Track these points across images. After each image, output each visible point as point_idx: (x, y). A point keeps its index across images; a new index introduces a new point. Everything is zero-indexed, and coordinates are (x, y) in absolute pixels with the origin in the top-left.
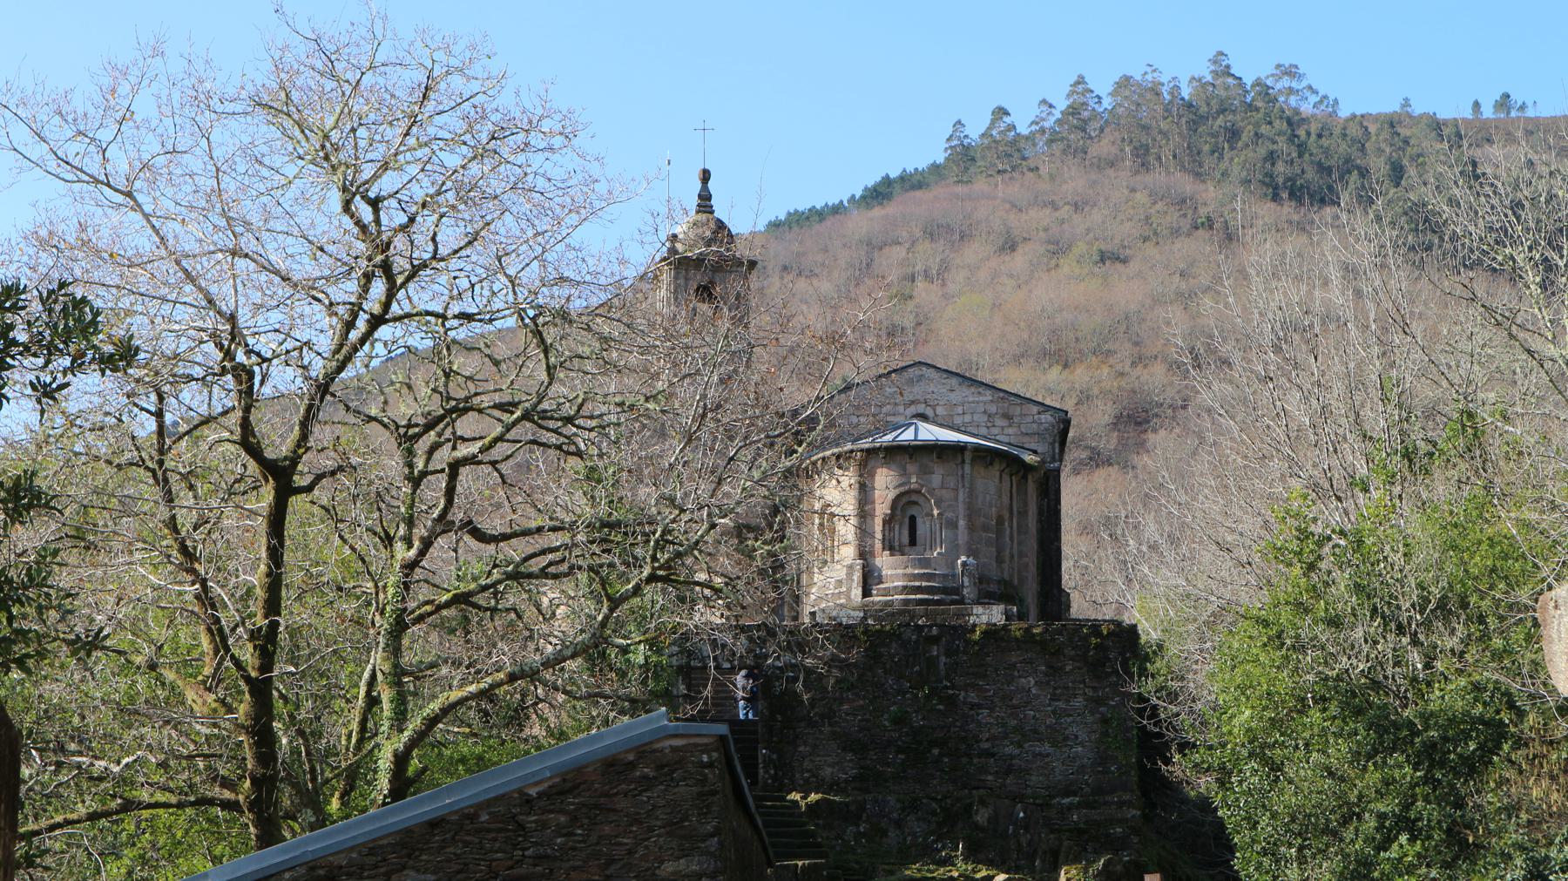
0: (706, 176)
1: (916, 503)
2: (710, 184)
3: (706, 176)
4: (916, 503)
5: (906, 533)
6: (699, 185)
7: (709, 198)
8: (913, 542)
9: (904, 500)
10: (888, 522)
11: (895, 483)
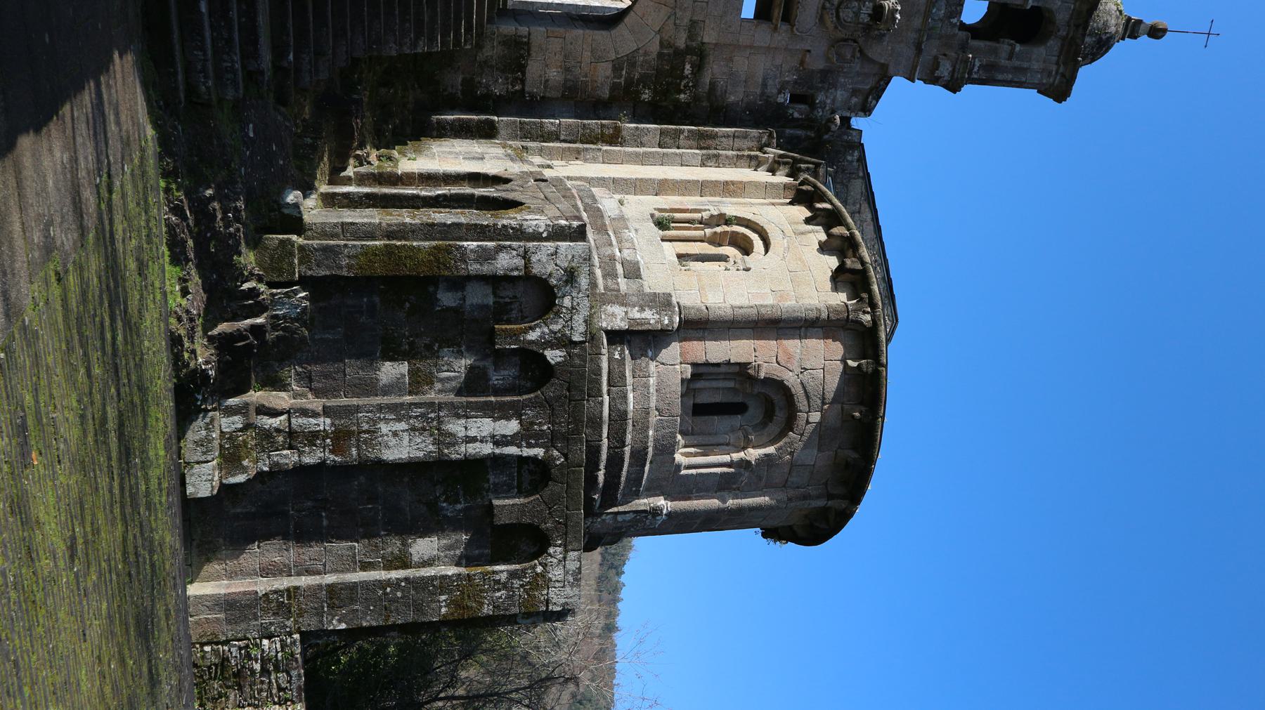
0: (1156, 32)
1: (769, 415)
2: (1144, 39)
3: (1156, 32)
4: (769, 415)
5: (718, 398)
6: (1149, 21)
7: (1134, 36)
9: (777, 398)
10: (741, 372)
11: (811, 386)
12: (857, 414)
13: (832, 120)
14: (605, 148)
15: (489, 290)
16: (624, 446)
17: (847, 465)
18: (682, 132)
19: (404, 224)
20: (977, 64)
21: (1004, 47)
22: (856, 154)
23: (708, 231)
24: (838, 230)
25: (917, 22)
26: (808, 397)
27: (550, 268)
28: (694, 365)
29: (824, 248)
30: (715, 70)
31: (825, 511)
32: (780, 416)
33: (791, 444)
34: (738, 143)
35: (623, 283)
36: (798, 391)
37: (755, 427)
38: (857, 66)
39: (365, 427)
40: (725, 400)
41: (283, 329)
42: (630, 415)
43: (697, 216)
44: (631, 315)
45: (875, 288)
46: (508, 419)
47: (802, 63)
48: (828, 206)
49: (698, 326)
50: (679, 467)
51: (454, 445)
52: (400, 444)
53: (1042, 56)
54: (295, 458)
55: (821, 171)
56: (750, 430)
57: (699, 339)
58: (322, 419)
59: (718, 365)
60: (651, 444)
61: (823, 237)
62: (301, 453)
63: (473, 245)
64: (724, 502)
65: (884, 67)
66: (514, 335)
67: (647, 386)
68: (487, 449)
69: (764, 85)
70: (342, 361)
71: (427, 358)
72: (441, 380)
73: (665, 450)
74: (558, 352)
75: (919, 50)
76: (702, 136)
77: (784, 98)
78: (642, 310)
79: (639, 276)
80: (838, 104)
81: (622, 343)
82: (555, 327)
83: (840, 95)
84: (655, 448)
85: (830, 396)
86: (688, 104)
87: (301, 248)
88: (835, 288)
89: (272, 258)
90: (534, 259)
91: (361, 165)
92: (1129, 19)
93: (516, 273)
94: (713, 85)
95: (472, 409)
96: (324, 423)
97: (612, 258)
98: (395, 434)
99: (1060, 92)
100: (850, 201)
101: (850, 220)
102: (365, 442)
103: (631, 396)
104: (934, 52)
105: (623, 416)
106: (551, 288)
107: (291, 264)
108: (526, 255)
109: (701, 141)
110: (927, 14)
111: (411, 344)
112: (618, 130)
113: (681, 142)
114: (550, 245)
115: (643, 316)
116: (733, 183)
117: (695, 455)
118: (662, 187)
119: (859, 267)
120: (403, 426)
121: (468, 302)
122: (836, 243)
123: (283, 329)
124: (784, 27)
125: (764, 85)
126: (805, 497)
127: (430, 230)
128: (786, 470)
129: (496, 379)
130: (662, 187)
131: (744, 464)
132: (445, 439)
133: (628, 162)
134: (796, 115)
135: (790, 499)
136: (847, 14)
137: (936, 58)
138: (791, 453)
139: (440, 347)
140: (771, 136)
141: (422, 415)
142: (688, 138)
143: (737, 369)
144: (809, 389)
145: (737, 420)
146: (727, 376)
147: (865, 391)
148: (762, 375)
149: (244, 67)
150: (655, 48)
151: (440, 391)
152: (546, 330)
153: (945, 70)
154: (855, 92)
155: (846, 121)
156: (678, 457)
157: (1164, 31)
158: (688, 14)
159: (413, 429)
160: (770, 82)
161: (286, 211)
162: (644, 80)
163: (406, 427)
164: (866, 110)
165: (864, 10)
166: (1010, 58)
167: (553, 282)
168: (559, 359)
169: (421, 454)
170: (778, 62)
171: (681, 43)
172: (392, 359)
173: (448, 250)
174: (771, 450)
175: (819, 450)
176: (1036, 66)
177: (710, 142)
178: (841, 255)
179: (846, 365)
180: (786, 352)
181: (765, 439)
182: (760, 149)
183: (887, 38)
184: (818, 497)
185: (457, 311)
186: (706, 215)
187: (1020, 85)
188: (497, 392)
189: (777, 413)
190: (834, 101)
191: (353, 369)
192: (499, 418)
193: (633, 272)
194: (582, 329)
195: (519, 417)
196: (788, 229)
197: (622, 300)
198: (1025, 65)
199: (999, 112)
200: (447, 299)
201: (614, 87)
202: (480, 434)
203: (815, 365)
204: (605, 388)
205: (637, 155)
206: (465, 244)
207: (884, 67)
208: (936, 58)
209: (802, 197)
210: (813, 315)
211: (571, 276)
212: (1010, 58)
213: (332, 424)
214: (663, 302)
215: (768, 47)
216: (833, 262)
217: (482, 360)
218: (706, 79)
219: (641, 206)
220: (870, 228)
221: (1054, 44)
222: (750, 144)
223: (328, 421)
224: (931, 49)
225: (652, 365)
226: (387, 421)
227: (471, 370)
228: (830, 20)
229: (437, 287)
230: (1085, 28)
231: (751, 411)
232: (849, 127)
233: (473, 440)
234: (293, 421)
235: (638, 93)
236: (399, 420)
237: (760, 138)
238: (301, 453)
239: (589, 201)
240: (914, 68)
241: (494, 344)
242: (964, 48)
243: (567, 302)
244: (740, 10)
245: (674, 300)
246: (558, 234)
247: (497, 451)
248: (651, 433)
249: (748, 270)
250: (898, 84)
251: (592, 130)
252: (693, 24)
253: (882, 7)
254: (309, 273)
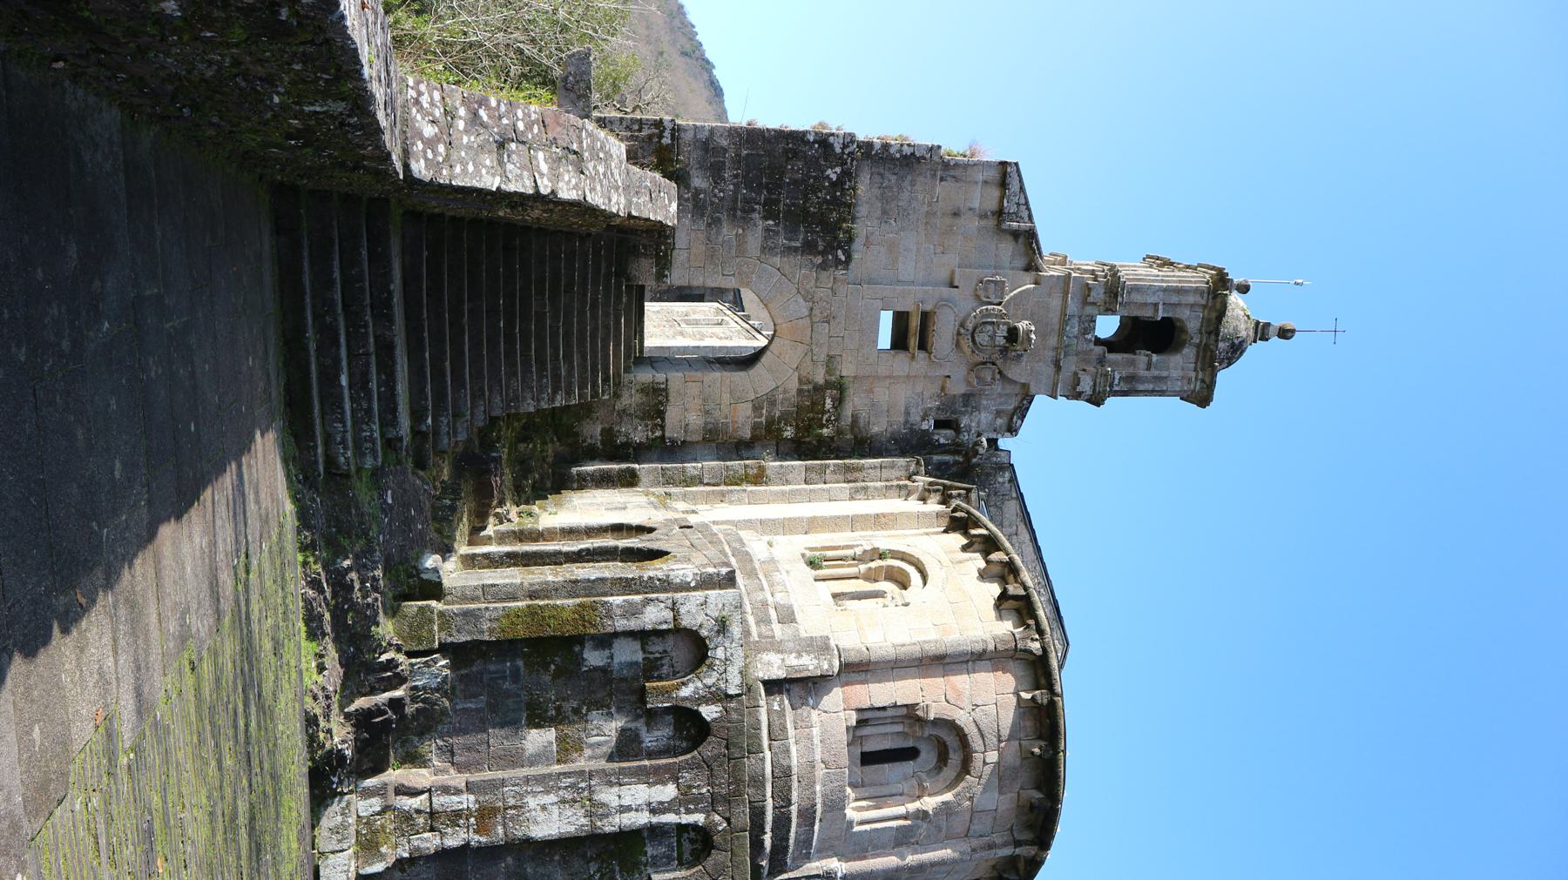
0: (1285, 333)
1: (943, 759)
2: (1275, 340)
3: (1285, 333)
4: (943, 759)
6: (1277, 323)
7: (1264, 338)
10: (910, 715)
12: (1036, 750)
13: (978, 443)
14: (751, 488)
15: (637, 645)
16: (790, 804)
17: (1032, 807)
18: (827, 466)
19: (547, 583)
20: (1117, 377)
21: (1142, 357)
22: (1007, 475)
23: (863, 567)
24: (996, 556)
25: (1053, 341)
26: (982, 736)
27: (701, 618)
28: (859, 710)
29: (983, 576)
30: (856, 402)
31: (1012, 861)
32: (955, 758)
33: (970, 788)
34: (886, 473)
35: (778, 630)
36: (971, 730)
37: (928, 773)
38: (998, 387)
39: (512, 802)
40: (895, 746)
41: (423, 701)
42: (795, 770)
43: (849, 552)
44: (788, 663)
45: (1041, 613)
46: (664, 783)
47: (943, 389)
48: (983, 531)
49: (857, 669)
50: (850, 823)
51: (607, 816)
52: (550, 820)
53: (1179, 364)
54: (437, 841)
55: (973, 496)
56: (924, 776)
57: (862, 683)
58: (465, 796)
59: (884, 708)
60: (819, 801)
61: (983, 564)
62: (443, 835)
63: (617, 600)
64: (903, 858)
65: (1025, 386)
66: (666, 692)
67: (810, 738)
68: (643, 818)
69: (907, 413)
70: (485, 731)
71: (574, 722)
72: (591, 746)
73: (835, 806)
74: (713, 707)
75: (1058, 368)
76: (848, 469)
77: (929, 425)
78: (799, 655)
79: (793, 620)
80: (983, 427)
81: (780, 693)
82: (709, 681)
83: (985, 417)
84: (824, 804)
85: (1005, 732)
86: (832, 438)
87: (441, 614)
88: (1000, 618)
89: (410, 626)
90: (683, 610)
91: (501, 523)
92: (1258, 323)
93: (665, 627)
94: (855, 418)
95: (625, 775)
96: (467, 801)
97: (765, 604)
98: (544, 808)
99: (1202, 398)
100: (1006, 523)
101: (1007, 544)
102: (512, 818)
103: (793, 749)
104: (1073, 368)
105: (787, 773)
106: (703, 640)
107: (431, 631)
108: (674, 607)
109: (849, 474)
110: (1062, 332)
111: (558, 709)
112: (762, 469)
113: (828, 477)
114: (699, 595)
115: (801, 662)
116: (884, 516)
117: (868, 808)
118: (812, 525)
119: (1022, 592)
120: (552, 798)
121: (616, 660)
122: (996, 569)
123: (423, 701)
124: (921, 355)
125: (907, 413)
126: (991, 846)
127: (574, 587)
128: (967, 817)
129: (650, 739)
130: (812, 525)
131: (922, 815)
132: (596, 810)
133: (774, 501)
134: (942, 441)
135: (974, 850)
136: (982, 338)
137: (1076, 374)
138: (971, 799)
139: (589, 710)
140: (918, 463)
141: (572, 786)
142: (834, 472)
143: (904, 711)
144: (982, 727)
145: (908, 767)
146: (894, 720)
147: (1043, 721)
148: (932, 716)
149: (382, 435)
150: (794, 385)
151: (590, 758)
152: (700, 685)
153: (1086, 385)
154: (999, 413)
155: (993, 443)
156: (851, 813)
157: (1293, 331)
158: (825, 350)
159: (563, 801)
160: (913, 410)
161: (425, 576)
162: (785, 417)
163: (556, 799)
164: (1012, 430)
165: (999, 333)
166: (1148, 369)
167: (704, 633)
168: (715, 715)
169: (572, 829)
170: (919, 389)
171: (820, 378)
172: (538, 726)
173: (593, 607)
174: (948, 797)
175: (1000, 793)
176: (1175, 374)
177: (857, 475)
178: (1003, 580)
179: (1019, 697)
180: (954, 689)
181: (941, 786)
182: (909, 478)
183: (1025, 359)
184: (1005, 845)
185: (604, 671)
186: (859, 551)
187: (1162, 393)
188: (651, 755)
189: (951, 755)
190: (978, 424)
191: (497, 738)
192: (656, 783)
193: (787, 617)
194: (737, 680)
195: (676, 779)
196: (945, 559)
197: (776, 646)
198: (1165, 374)
199: (1145, 420)
200: (594, 658)
201: (755, 427)
202: (635, 802)
203: (986, 703)
204: (765, 742)
205: (783, 493)
206: (610, 599)
207: (1025, 386)
208: (1076, 374)
209: (958, 524)
210: (979, 647)
211: (722, 626)
212: (1148, 369)
213: (477, 801)
214: (821, 646)
215: (908, 377)
216: (995, 589)
217: (634, 721)
218: (848, 411)
219: (791, 548)
220: (1029, 549)
221: (1189, 352)
222: (898, 474)
223: (472, 798)
224: (1070, 366)
225: (814, 713)
226: (535, 794)
227: (623, 732)
228: (966, 344)
229: (583, 647)
230: (1217, 335)
231: (923, 755)
232: (997, 449)
233: (628, 809)
234: (434, 799)
235: (780, 430)
236: (547, 792)
237: (908, 466)
238: (443, 835)
239: (737, 545)
240: (1055, 385)
241: (645, 703)
242: (1101, 361)
243: (720, 653)
244: (876, 342)
245: (832, 644)
246: (707, 583)
247: (655, 820)
248: (818, 788)
249: (906, 605)
250: (1041, 402)
251: (736, 472)
252: (830, 358)
253: (1016, 329)
254: (449, 640)
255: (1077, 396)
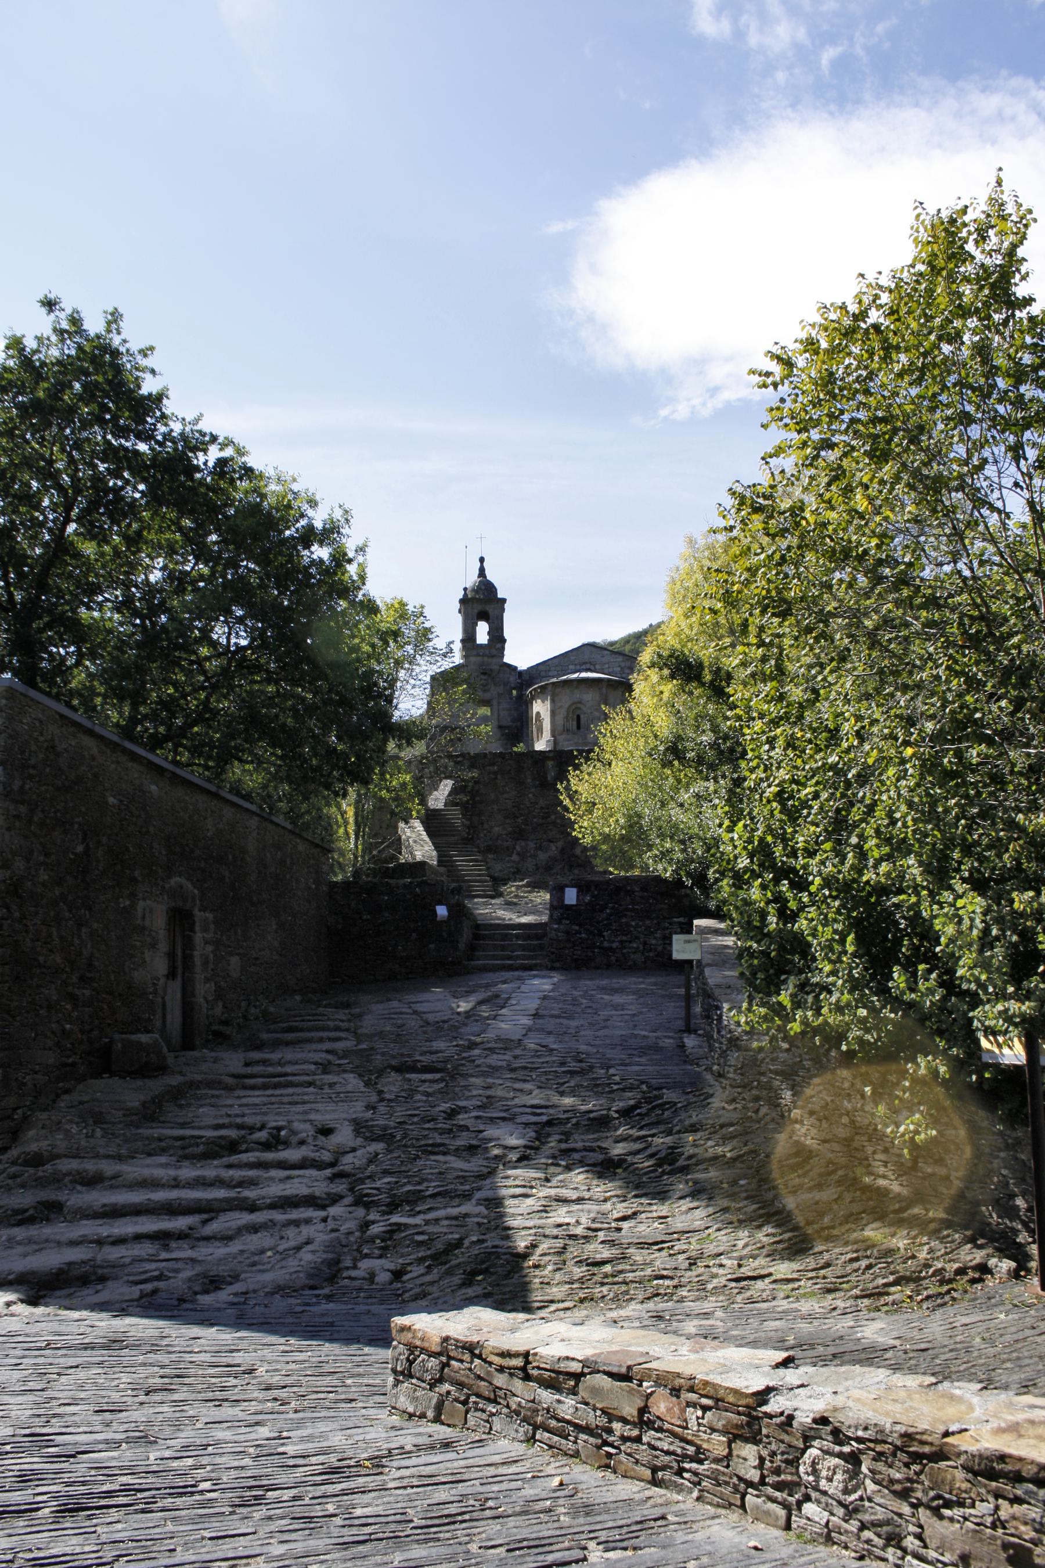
0: (482, 560)
3: (482, 560)
8: (579, 727)
36: (569, 703)
83: (512, 679)
99: (504, 601)
153: (499, 646)
224: (494, 652)
250: (506, 660)
255: (503, 649)
